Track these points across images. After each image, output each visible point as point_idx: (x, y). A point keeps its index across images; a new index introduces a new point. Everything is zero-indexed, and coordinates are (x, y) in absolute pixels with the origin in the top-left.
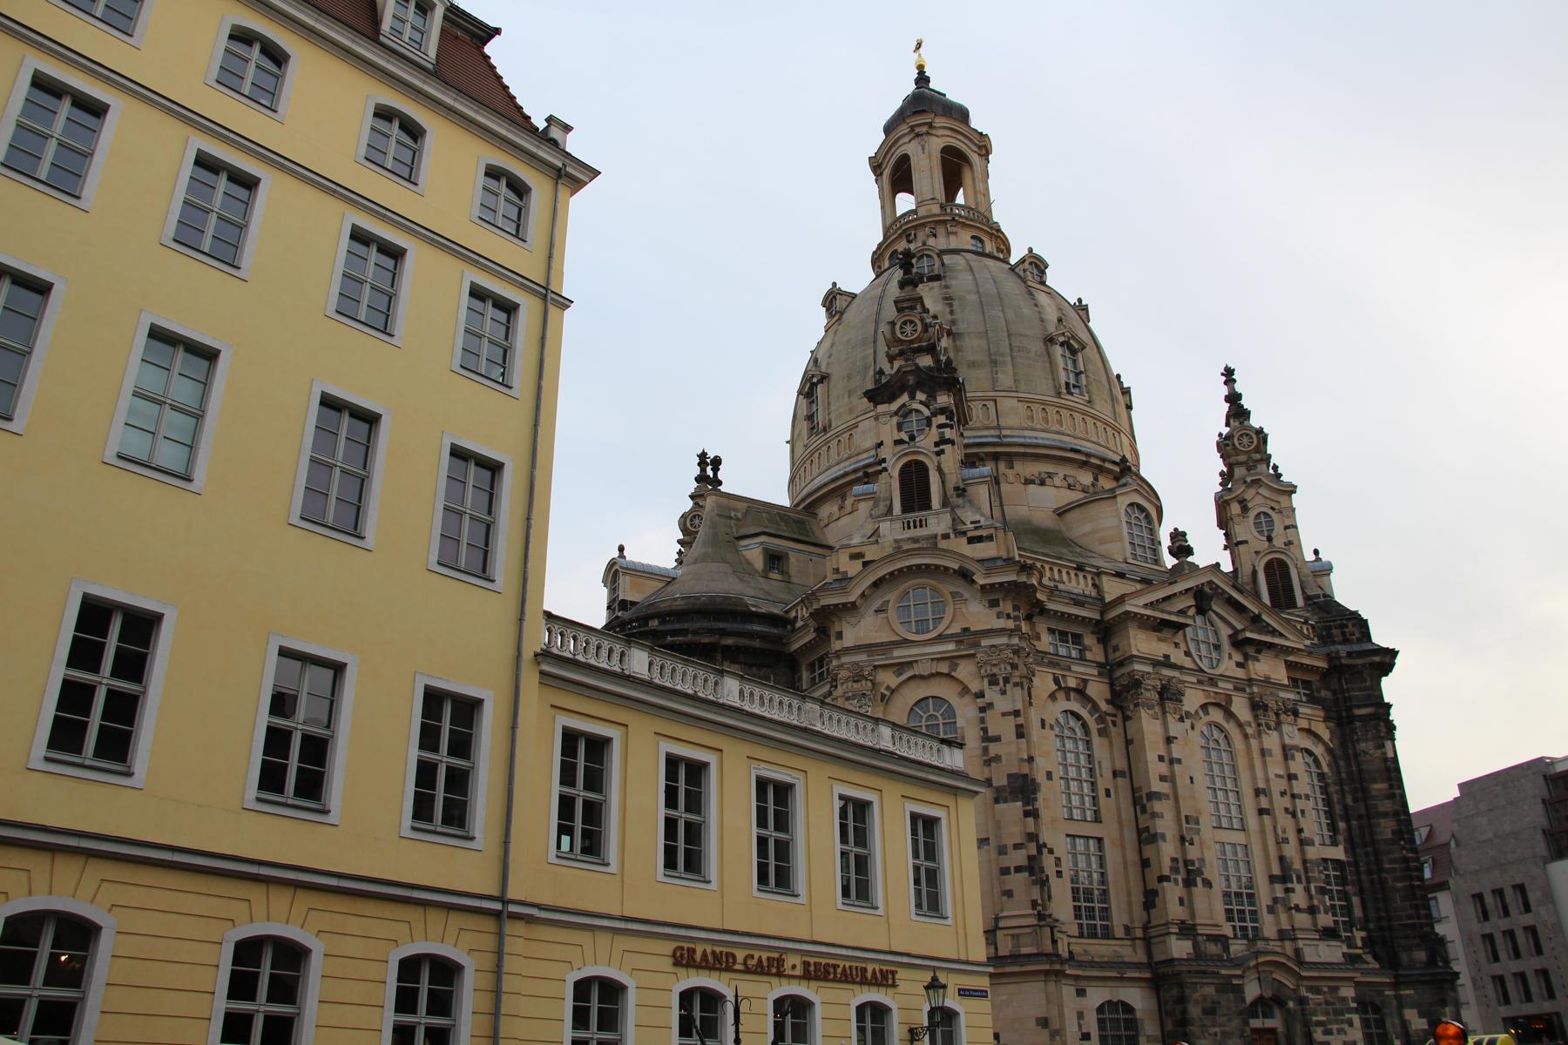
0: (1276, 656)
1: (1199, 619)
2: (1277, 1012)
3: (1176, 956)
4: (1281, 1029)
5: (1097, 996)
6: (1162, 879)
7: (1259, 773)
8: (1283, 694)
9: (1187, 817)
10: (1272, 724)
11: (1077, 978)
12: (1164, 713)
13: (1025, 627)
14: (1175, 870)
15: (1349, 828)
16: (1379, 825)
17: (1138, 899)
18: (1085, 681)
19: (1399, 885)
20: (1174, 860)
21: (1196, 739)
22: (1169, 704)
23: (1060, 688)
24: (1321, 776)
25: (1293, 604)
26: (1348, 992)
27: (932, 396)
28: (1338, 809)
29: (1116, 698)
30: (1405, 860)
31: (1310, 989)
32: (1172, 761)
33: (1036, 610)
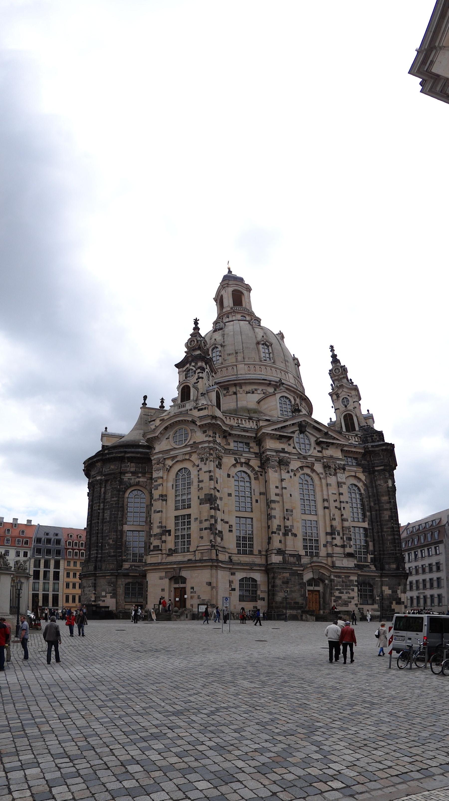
1: (301, 436)
6: (273, 533)
7: (325, 493)
8: (338, 462)
9: (287, 510)
12: (281, 470)
13: (218, 440)
18: (249, 460)
22: (282, 467)
32: (282, 488)
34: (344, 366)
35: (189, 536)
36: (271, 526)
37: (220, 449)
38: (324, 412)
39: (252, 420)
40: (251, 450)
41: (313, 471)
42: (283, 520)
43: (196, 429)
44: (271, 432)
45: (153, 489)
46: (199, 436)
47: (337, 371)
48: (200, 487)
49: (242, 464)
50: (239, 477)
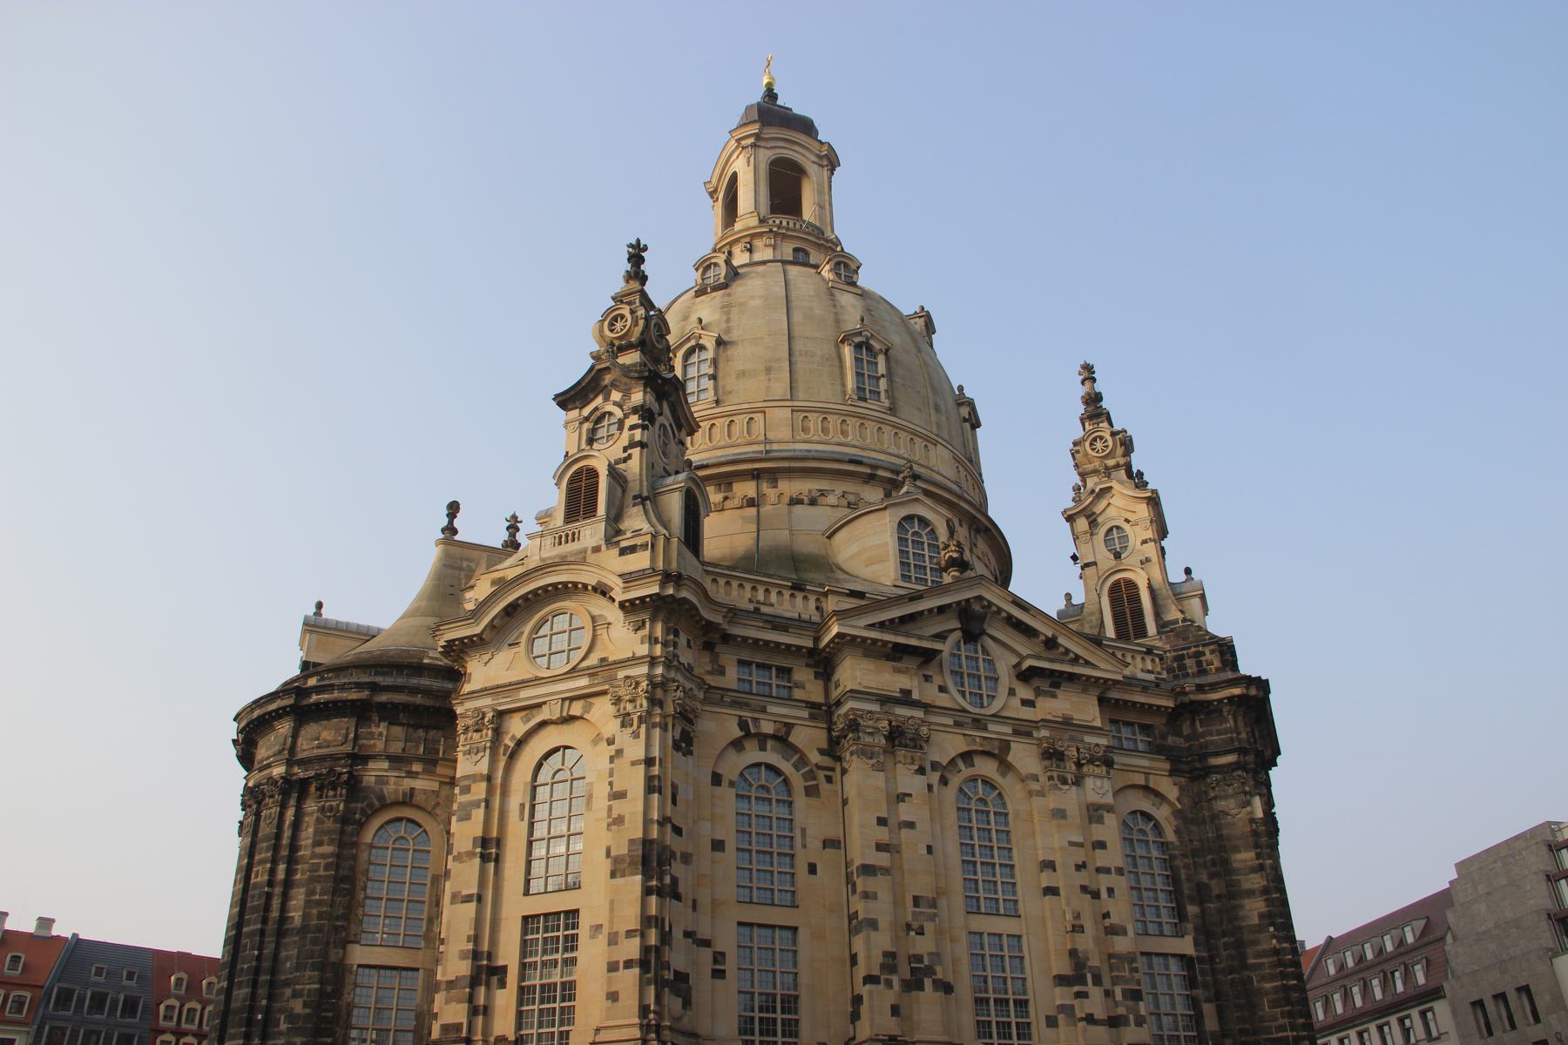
0: (1085, 691)
6: (870, 979)
8: (1088, 739)
10: (1069, 777)
13: (686, 657)
15: (1203, 912)
16: (1241, 907)
19: (1268, 986)
21: (950, 793)
22: (901, 753)
23: (748, 735)
24: (1164, 846)
25: (1141, 631)
27: (627, 394)
29: (833, 750)
30: (1276, 952)
35: (569, 989)
36: (861, 958)
37: (688, 685)
39: (803, 590)
40: (798, 694)
42: (902, 934)
44: (865, 634)
45: (454, 819)
49: (762, 739)
50: (750, 785)
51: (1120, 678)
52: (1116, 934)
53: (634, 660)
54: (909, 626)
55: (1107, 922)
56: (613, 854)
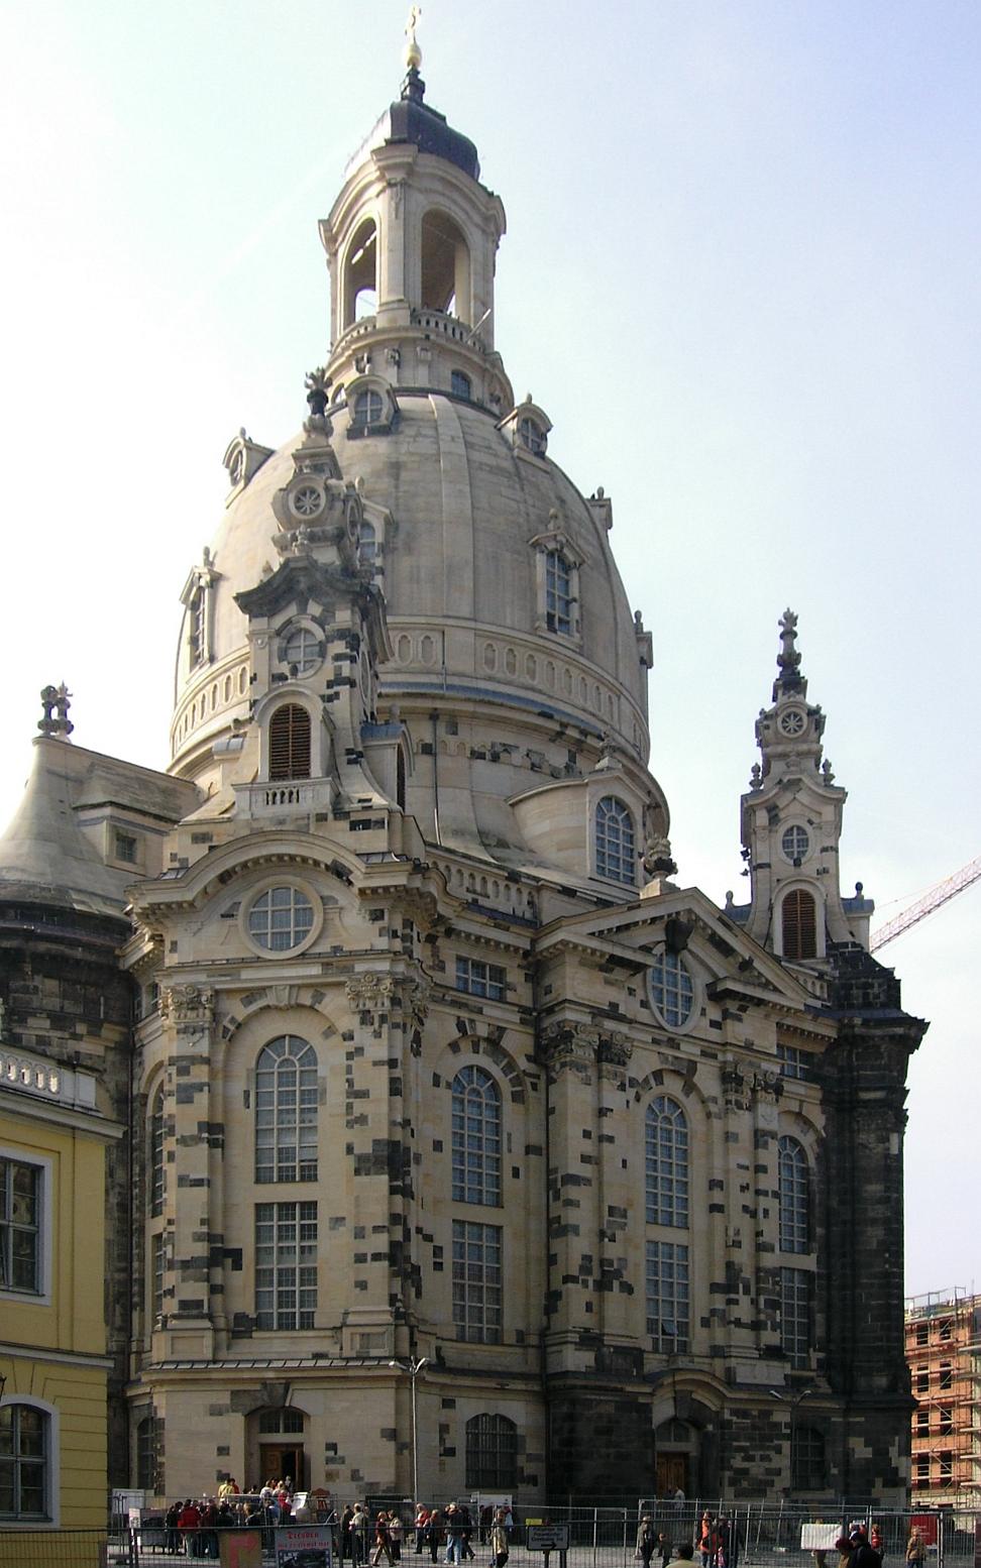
2: (693, 1435)
3: (572, 1368)
4: (694, 1454)
5: (469, 1407)
6: (567, 1279)
8: (765, 1066)
9: (610, 1208)
10: (745, 1102)
11: (444, 1386)
12: (600, 1077)
13: (420, 951)
14: (586, 1269)
17: (538, 1300)
18: (501, 1030)
20: (587, 1258)
21: (640, 1110)
22: (606, 1066)
26: (782, 1417)
28: (818, 1212)
31: (734, 1412)
32: (602, 1139)
33: (440, 929)
34: (819, 708)
36: (561, 1259)
38: (710, 861)
39: (516, 881)
41: (690, 1087)
42: (596, 1240)
43: (347, 899)
46: (355, 928)
47: (792, 723)
48: (357, 1112)
50: (464, 1087)
51: (802, 1008)
52: (766, 1250)
53: (371, 953)
54: (623, 937)
55: (761, 1239)
56: (356, 1151)
